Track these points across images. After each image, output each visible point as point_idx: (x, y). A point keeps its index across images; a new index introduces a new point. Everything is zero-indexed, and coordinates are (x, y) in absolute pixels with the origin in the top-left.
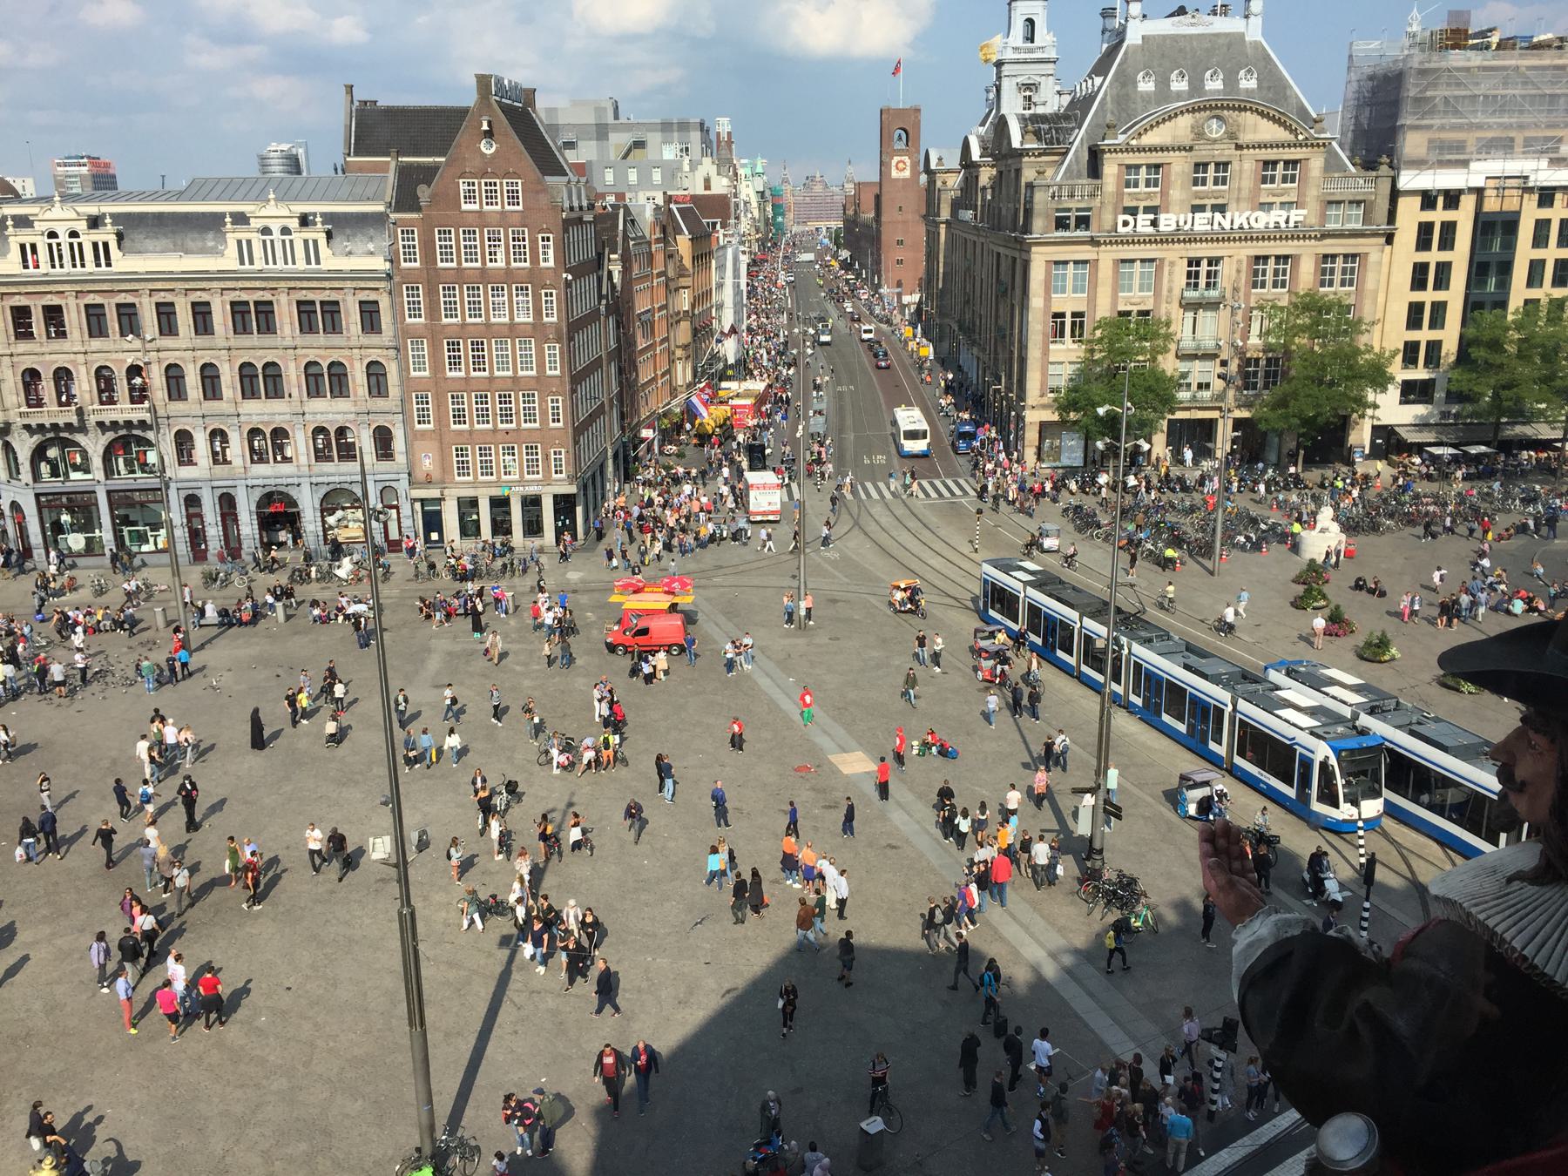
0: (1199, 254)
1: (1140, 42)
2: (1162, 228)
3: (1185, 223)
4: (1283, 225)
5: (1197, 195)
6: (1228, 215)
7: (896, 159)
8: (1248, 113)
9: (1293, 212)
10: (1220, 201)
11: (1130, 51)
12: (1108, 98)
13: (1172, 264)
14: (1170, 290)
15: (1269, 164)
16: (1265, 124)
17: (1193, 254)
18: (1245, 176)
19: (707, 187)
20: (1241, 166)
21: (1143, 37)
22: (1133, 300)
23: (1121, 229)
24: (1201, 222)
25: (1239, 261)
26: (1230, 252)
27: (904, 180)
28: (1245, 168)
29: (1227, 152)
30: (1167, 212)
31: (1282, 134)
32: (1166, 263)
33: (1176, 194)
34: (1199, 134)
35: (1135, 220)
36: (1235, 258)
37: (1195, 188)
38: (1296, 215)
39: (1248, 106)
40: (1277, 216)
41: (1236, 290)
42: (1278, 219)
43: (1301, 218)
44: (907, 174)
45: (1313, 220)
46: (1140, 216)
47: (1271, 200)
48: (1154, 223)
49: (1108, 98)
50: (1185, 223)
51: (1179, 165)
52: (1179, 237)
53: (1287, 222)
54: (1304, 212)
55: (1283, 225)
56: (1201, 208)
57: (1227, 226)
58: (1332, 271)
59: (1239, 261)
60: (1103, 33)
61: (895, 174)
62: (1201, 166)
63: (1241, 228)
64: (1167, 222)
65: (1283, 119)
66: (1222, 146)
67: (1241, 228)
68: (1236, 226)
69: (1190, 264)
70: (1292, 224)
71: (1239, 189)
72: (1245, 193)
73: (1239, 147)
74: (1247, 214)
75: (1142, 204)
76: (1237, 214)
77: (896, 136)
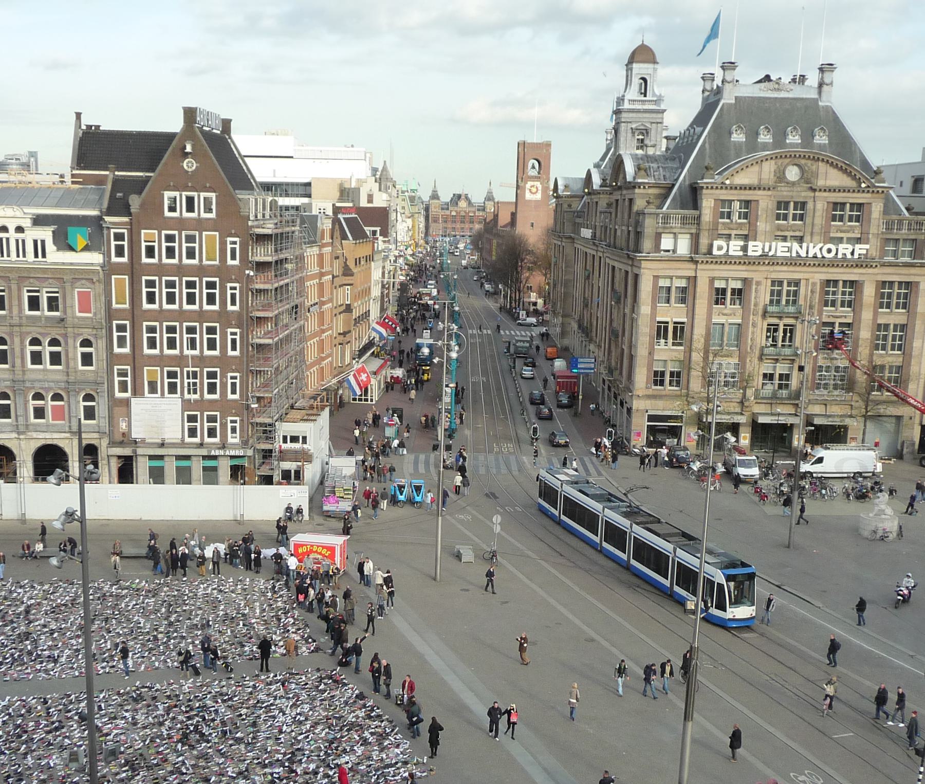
0: (781, 276)
1: (733, 101)
2: (750, 253)
3: (770, 250)
4: (849, 256)
5: (779, 228)
6: (805, 245)
7: (529, 184)
8: (820, 163)
9: (858, 246)
10: (798, 234)
11: (725, 107)
12: (707, 145)
13: (758, 283)
14: (755, 305)
15: (836, 205)
16: (833, 172)
17: (774, 276)
18: (818, 214)
19: (370, 200)
21: (736, 98)
22: (725, 312)
23: (715, 252)
24: (780, 249)
25: (814, 284)
26: (806, 276)
27: (536, 201)
28: (819, 207)
29: (803, 194)
30: (755, 240)
31: (848, 182)
32: (754, 283)
33: (761, 226)
34: (781, 177)
35: (728, 245)
36: (811, 281)
37: (777, 222)
38: (860, 249)
39: (821, 157)
40: (845, 249)
41: (811, 307)
42: (844, 252)
43: (864, 252)
44: (538, 196)
45: (874, 253)
46: (732, 243)
47: (840, 235)
48: (745, 249)
49: (707, 145)
50: (770, 250)
51: (765, 202)
52: (765, 259)
53: (852, 253)
54: (867, 246)
55: (849, 256)
56: (785, 239)
57: (803, 254)
58: (890, 296)
59: (814, 284)
60: (703, 92)
61: (528, 196)
62: (782, 205)
63: (815, 257)
64: (755, 248)
65: (849, 169)
66: (799, 189)
67: (815, 257)
68: (810, 255)
69: (773, 283)
70: (856, 256)
74: (821, 245)
75: (733, 233)
76: (811, 245)
77: (530, 165)
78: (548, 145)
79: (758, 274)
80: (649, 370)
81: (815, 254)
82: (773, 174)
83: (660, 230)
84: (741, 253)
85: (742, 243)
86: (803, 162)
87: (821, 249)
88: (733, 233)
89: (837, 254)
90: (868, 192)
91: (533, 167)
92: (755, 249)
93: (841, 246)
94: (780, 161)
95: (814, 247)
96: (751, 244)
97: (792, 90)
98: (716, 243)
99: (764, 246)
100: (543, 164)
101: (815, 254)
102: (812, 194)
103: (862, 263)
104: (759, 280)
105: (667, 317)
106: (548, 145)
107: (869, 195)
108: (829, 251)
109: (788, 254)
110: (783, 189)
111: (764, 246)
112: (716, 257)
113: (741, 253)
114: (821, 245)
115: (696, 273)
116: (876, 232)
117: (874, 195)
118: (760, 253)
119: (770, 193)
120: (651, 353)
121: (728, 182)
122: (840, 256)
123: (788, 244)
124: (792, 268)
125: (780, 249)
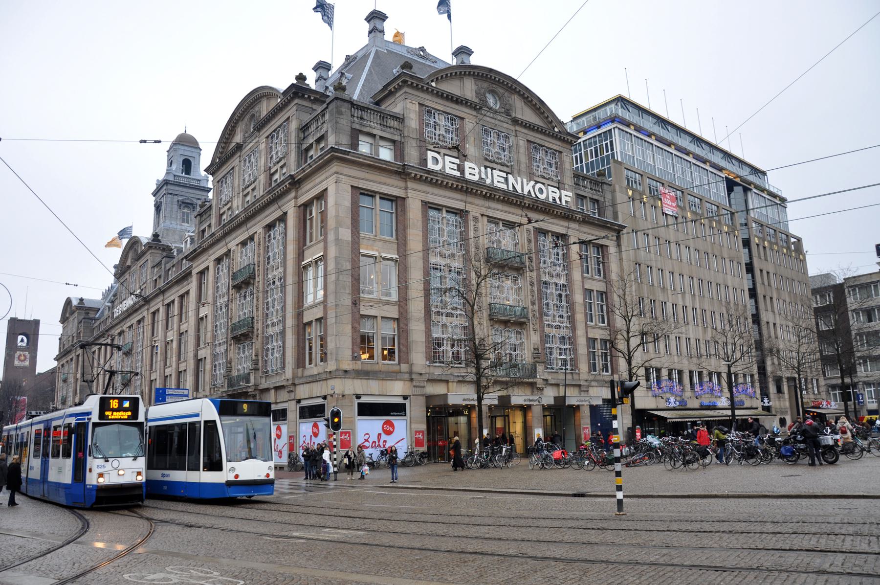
4: (558, 202)
6: (519, 179)
7: (18, 353)
8: (516, 97)
13: (475, 219)
14: (477, 248)
20: (517, 141)
23: (431, 165)
24: (496, 179)
27: (24, 368)
32: (471, 217)
33: (471, 149)
38: (567, 197)
43: (569, 199)
48: (461, 168)
54: (570, 194)
55: (558, 202)
57: (519, 190)
61: (17, 363)
64: (473, 172)
66: (500, 118)
68: (526, 193)
70: (564, 203)
71: (519, 162)
72: (523, 167)
73: (515, 121)
74: (532, 183)
78: (36, 323)
79: (476, 207)
80: (355, 329)
81: (529, 192)
82: (474, 94)
83: (357, 127)
84: (458, 174)
85: (457, 161)
86: (500, 91)
87: (534, 187)
88: (443, 151)
89: (548, 197)
90: (560, 139)
91: (22, 341)
92: (472, 171)
93: (551, 189)
94: (479, 83)
95: (527, 184)
96: (467, 165)
97: (436, 62)
98: (430, 154)
99: (480, 170)
100: (31, 337)
101: (529, 192)
102: (512, 128)
103: (566, 215)
104: (476, 215)
105: (373, 250)
106: (36, 323)
107: (559, 143)
108: (541, 191)
109: (504, 186)
110: (488, 114)
111: (480, 170)
112: (430, 172)
113: (458, 174)
114: (532, 183)
115: (407, 192)
116: (570, 184)
117: (564, 145)
118: (476, 178)
119: (474, 113)
120: (355, 303)
121: (433, 84)
122: (551, 200)
123: (504, 175)
124: (506, 208)
125: (496, 179)
